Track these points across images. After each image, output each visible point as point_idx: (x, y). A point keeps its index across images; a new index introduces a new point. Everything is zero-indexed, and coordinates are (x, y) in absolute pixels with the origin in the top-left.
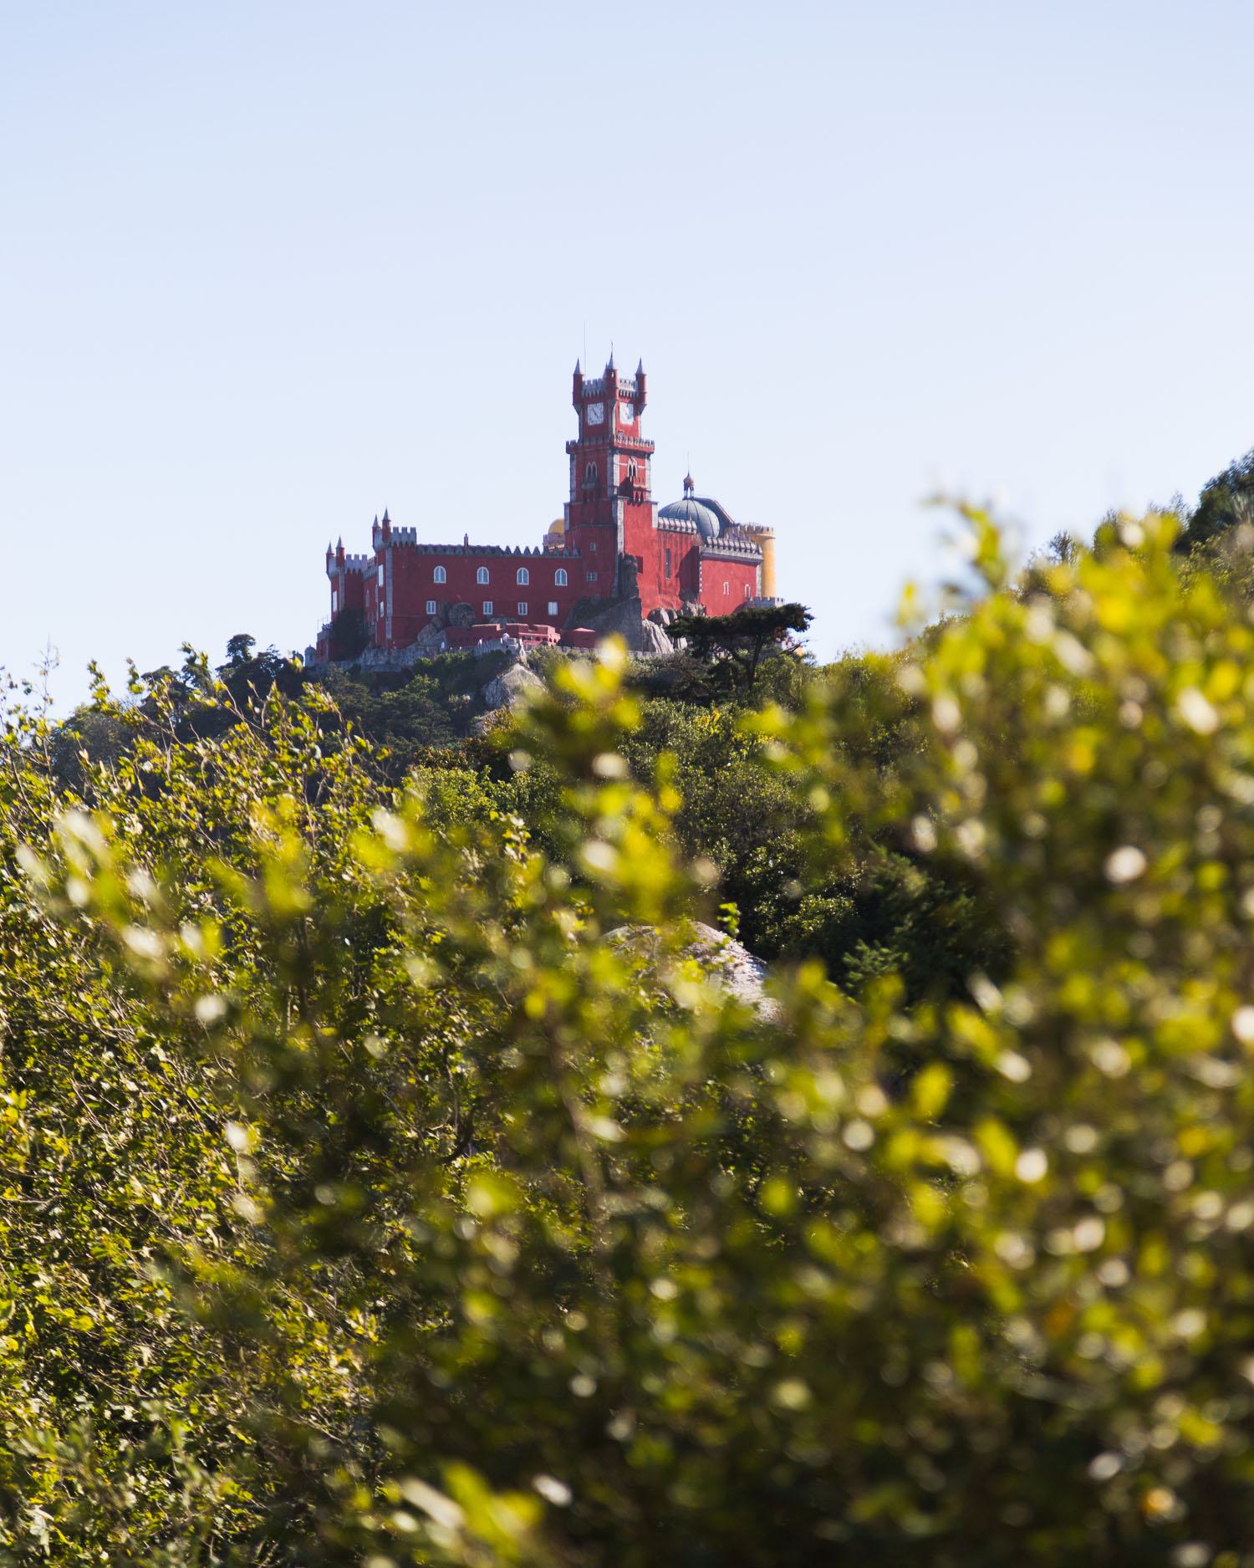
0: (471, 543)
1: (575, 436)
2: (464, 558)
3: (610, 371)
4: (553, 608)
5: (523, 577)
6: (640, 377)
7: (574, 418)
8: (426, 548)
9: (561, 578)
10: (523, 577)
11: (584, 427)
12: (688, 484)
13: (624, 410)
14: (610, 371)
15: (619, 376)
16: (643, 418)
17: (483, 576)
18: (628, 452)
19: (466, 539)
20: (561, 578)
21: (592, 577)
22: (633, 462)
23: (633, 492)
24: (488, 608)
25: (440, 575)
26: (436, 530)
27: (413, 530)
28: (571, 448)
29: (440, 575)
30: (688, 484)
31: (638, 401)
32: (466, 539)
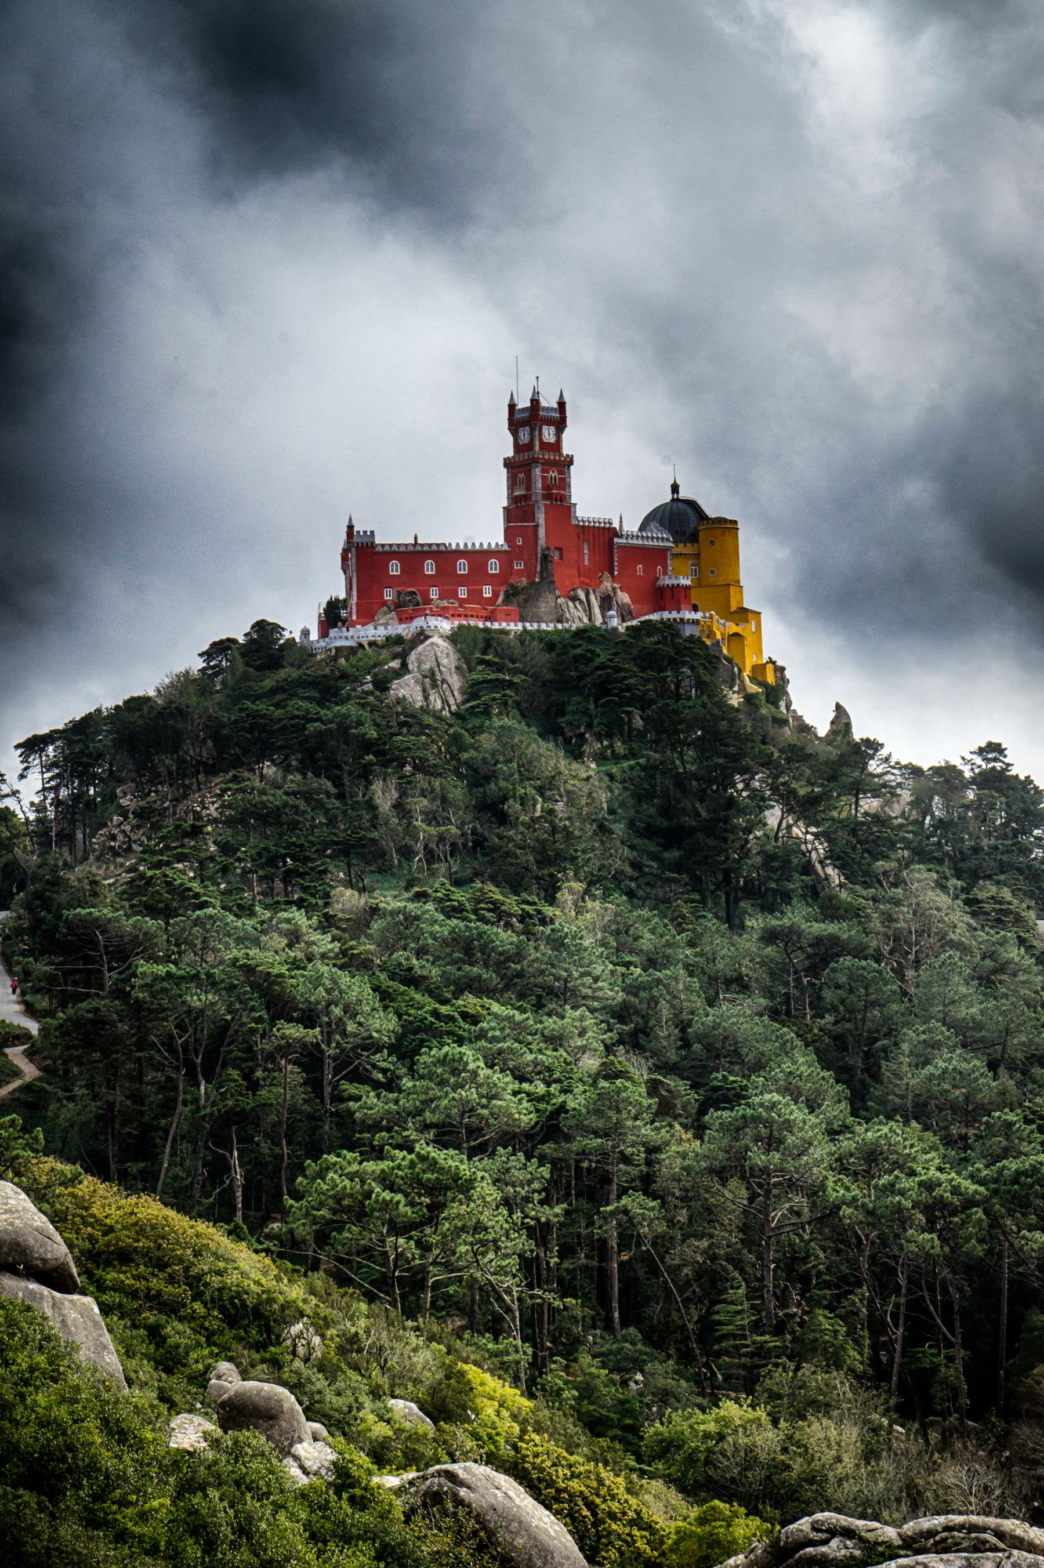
0: (420, 541)
1: (510, 453)
2: (413, 556)
3: (535, 402)
4: (487, 592)
5: (462, 567)
6: (562, 405)
7: (511, 438)
8: (383, 546)
9: (494, 567)
10: (462, 567)
11: (518, 447)
12: (675, 488)
13: (548, 434)
14: (535, 402)
15: (544, 403)
16: (565, 436)
17: (429, 568)
18: (547, 465)
19: (416, 538)
20: (494, 567)
21: (519, 566)
22: (553, 474)
23: (558, 497)
24: (434, 594)
25: (395, 568)
26: (391, 534)
27: (372, 532)
28: (508, 463)
29: (395, 568)
30: (675, 488)
31: (560, 425)
32: (416, 538)
